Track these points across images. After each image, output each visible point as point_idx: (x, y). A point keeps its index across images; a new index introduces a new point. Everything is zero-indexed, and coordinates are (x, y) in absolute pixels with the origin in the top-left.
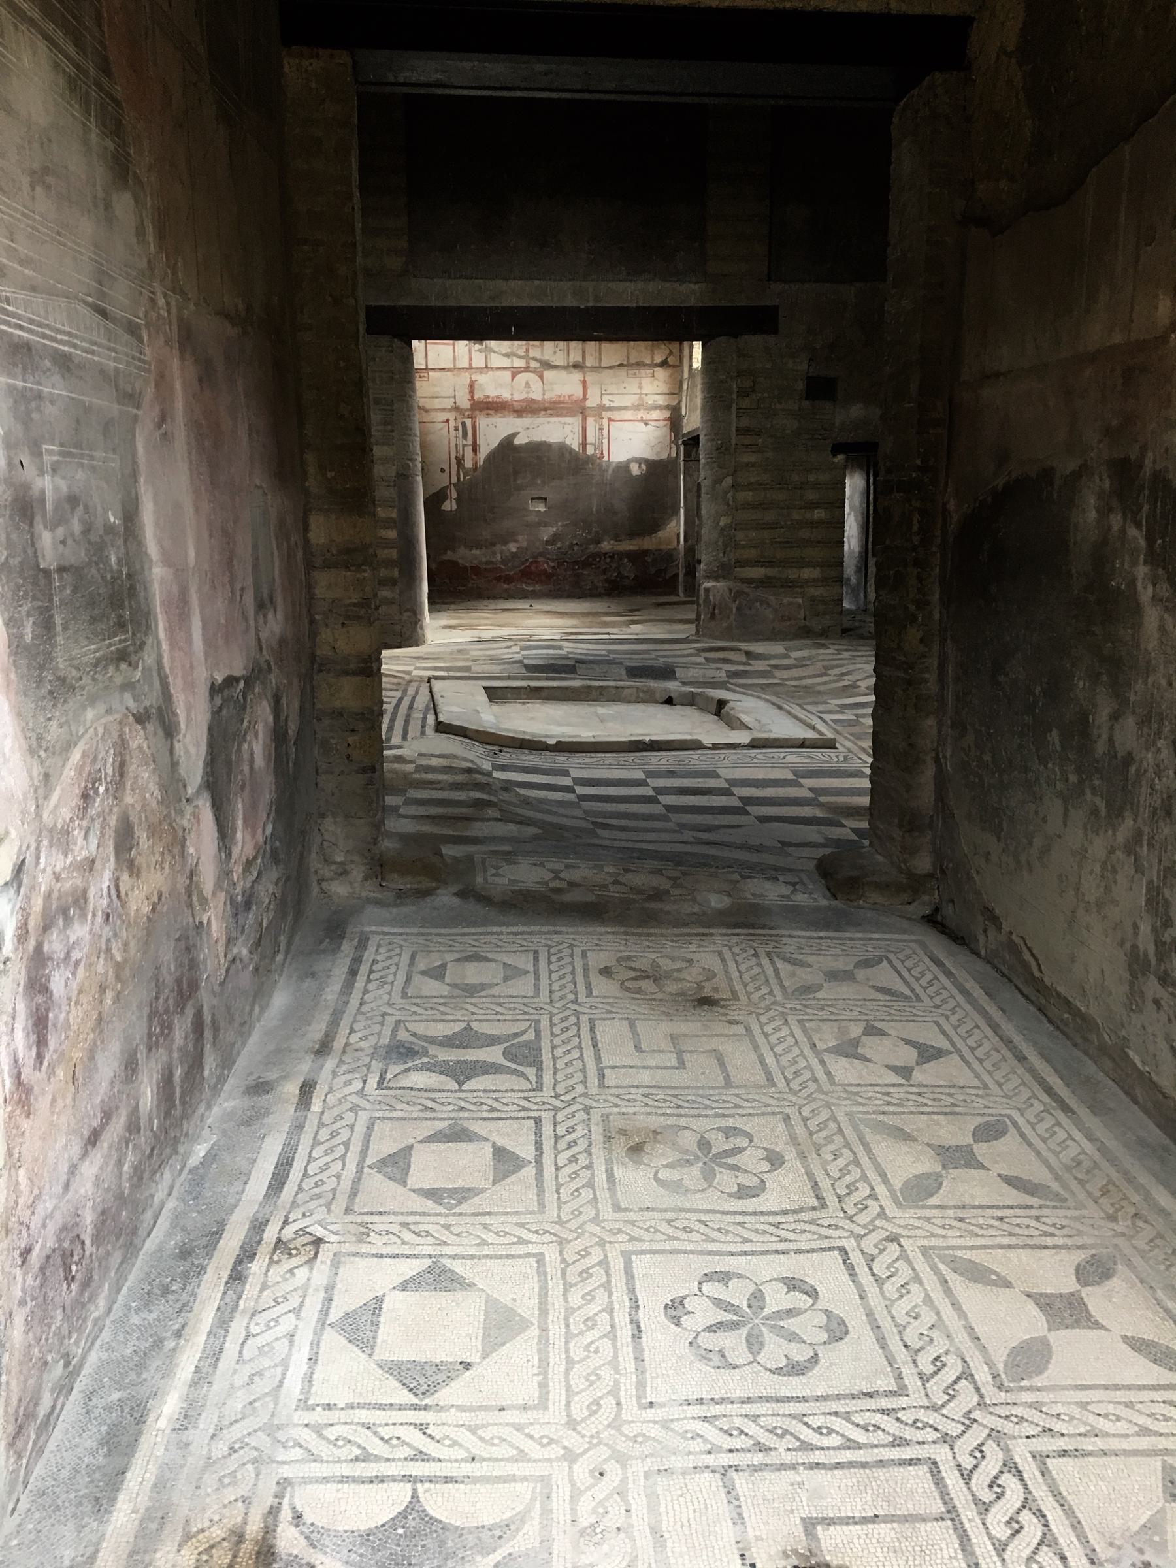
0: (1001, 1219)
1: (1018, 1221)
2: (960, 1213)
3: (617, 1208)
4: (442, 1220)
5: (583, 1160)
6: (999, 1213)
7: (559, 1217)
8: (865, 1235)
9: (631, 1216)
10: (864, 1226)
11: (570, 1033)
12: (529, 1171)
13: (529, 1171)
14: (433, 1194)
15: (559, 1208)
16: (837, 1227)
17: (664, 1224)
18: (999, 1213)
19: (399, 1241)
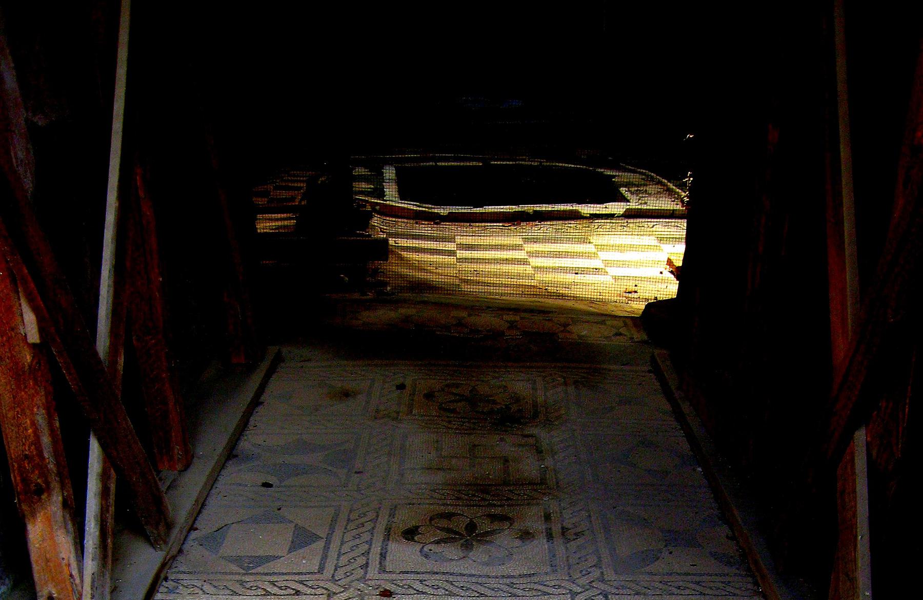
0: (698, 583)
1: (712, 585)
2: (666, 579)
3: (382, 570)
4: (238, 577)
5: (367, 537)
6: (697, 579)
7: (333, 576)
8: (581, 592)
9: (394, 576)
10: (583, 587)
11: (385, 443)
12: (320, 544)
13: (320, 544)
14: (237, 560)
15: (336, 570)
16: (560, 587)
17: (418, 582)
18: (697, 579)
19: (201, 592)
